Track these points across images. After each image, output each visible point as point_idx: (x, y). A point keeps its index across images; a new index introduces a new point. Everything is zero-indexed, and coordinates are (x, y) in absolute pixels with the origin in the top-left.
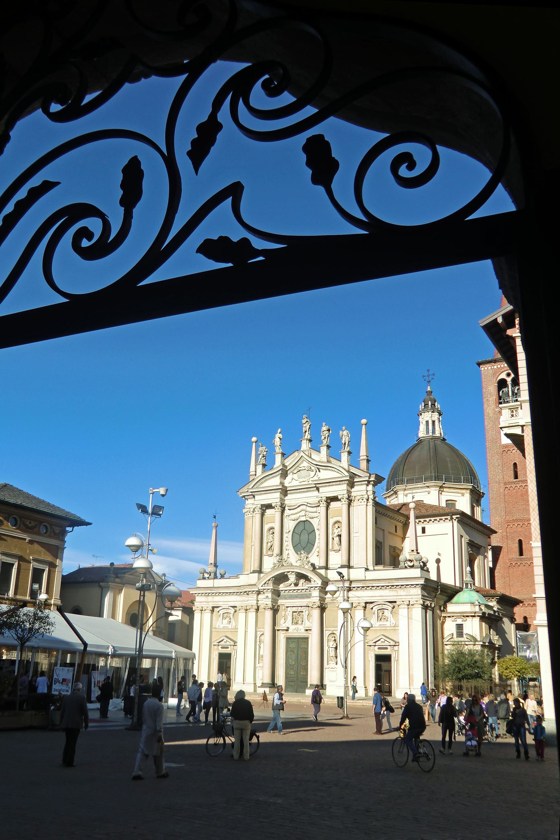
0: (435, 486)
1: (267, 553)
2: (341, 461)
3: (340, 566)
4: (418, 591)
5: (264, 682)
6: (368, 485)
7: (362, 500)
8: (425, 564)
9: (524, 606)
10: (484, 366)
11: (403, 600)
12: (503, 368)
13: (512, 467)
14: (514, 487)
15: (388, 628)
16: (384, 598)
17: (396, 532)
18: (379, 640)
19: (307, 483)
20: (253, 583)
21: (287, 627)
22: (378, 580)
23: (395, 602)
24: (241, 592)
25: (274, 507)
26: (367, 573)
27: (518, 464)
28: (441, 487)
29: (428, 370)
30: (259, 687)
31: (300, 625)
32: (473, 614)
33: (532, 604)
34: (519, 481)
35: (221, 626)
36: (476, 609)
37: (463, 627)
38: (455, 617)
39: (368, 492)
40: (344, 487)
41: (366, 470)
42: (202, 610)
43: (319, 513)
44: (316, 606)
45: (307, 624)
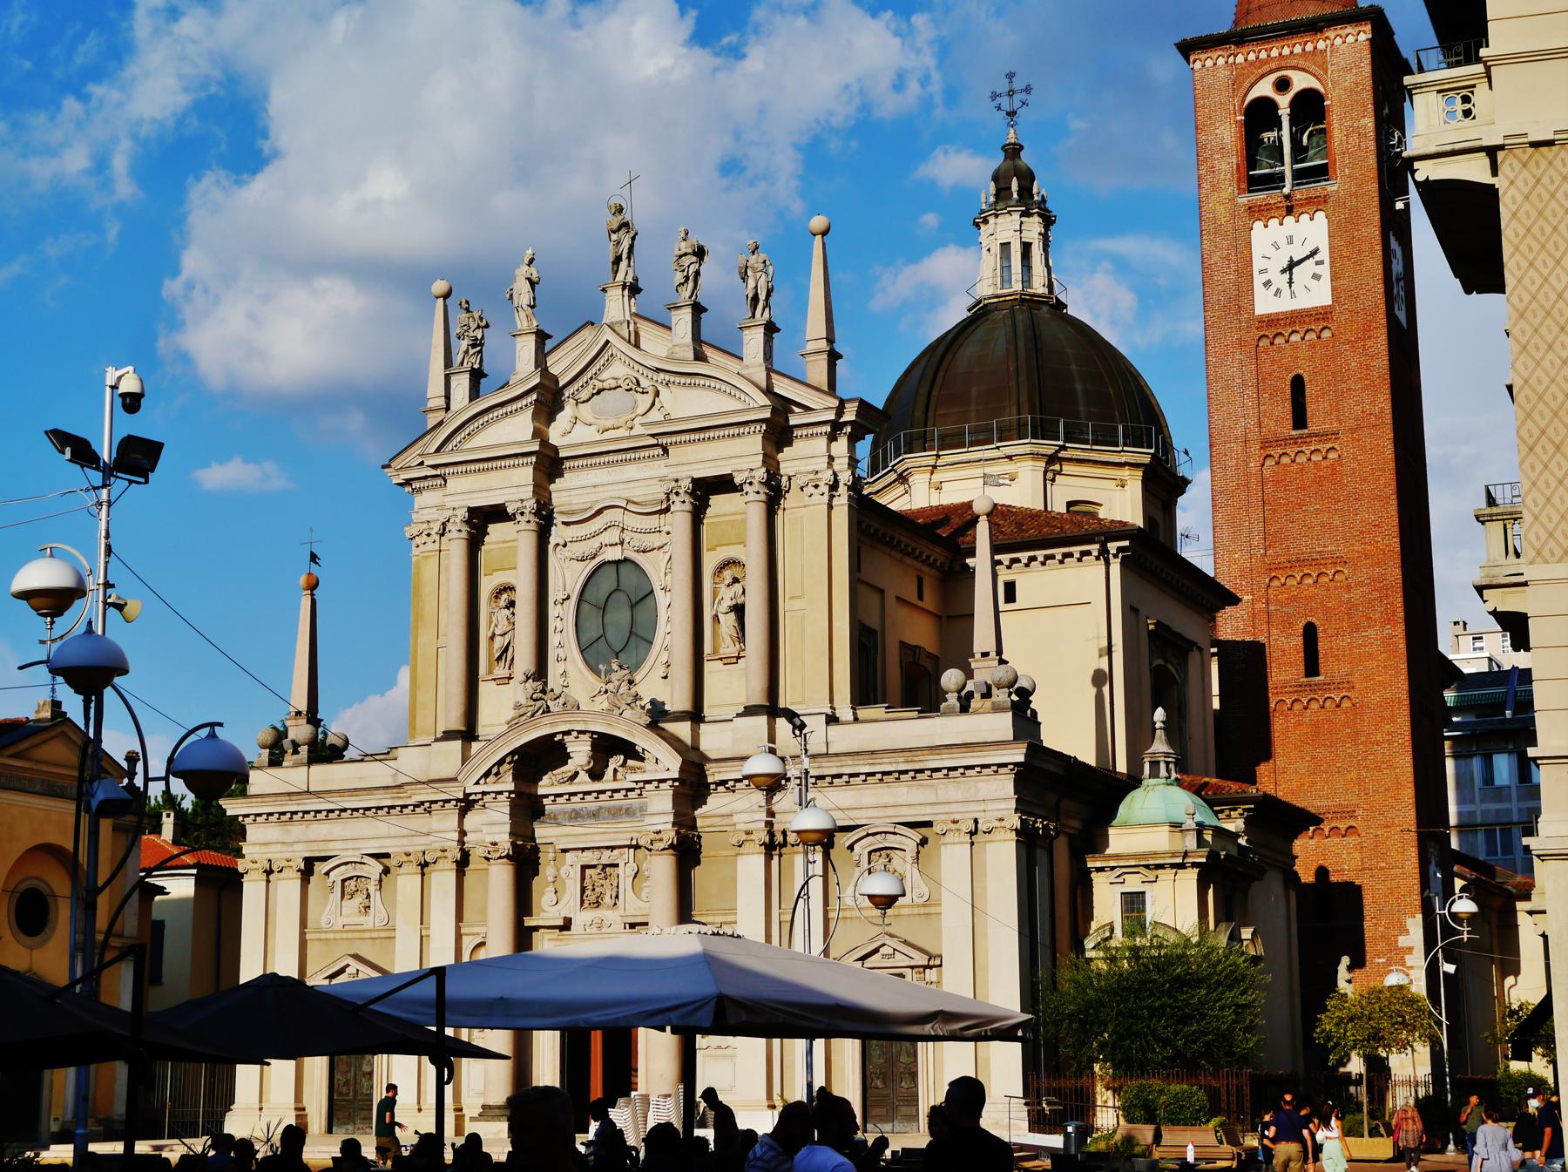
0: (1035, 456)
1: (490, 672)
2: (741, 359)
3: (741, 710)
4: (1004, 786)
5: (491, 1102)
6: (832, 438)
7: (816, 486)
8: (1025, 694)
9: (1321, 834)
10: (1203, 56)
11: (957, 817)
12: (1265, 62)
13: (1288, 391)
14: (1293, 455)
16: (891, 812)
17: (921, 597)
18: (876, 951)
19: (626, 434)
20: (444, 775)
21: (565, 918)
22: (873, 752)
23: (929, 824)
24: (406, 806)
25: (514, 514)
26: (833, 729)
27: (1306, 379)
28: (1052, 459)
29: (1010, 76)
30: (472, 1119)
31: (608, 908)
32: (1179, 860)
33: (1343, 826)
34: (1310, 436)
35: (340, 922)
36: (1187, 844)
37: (1144, 902)
38: (1118, 872)
39: (837, 461)
40: (753, 444)
41: (826, 388)
42: (269, 872)
43: (668, 533)
44: (661, 845)
45: (632, 906)
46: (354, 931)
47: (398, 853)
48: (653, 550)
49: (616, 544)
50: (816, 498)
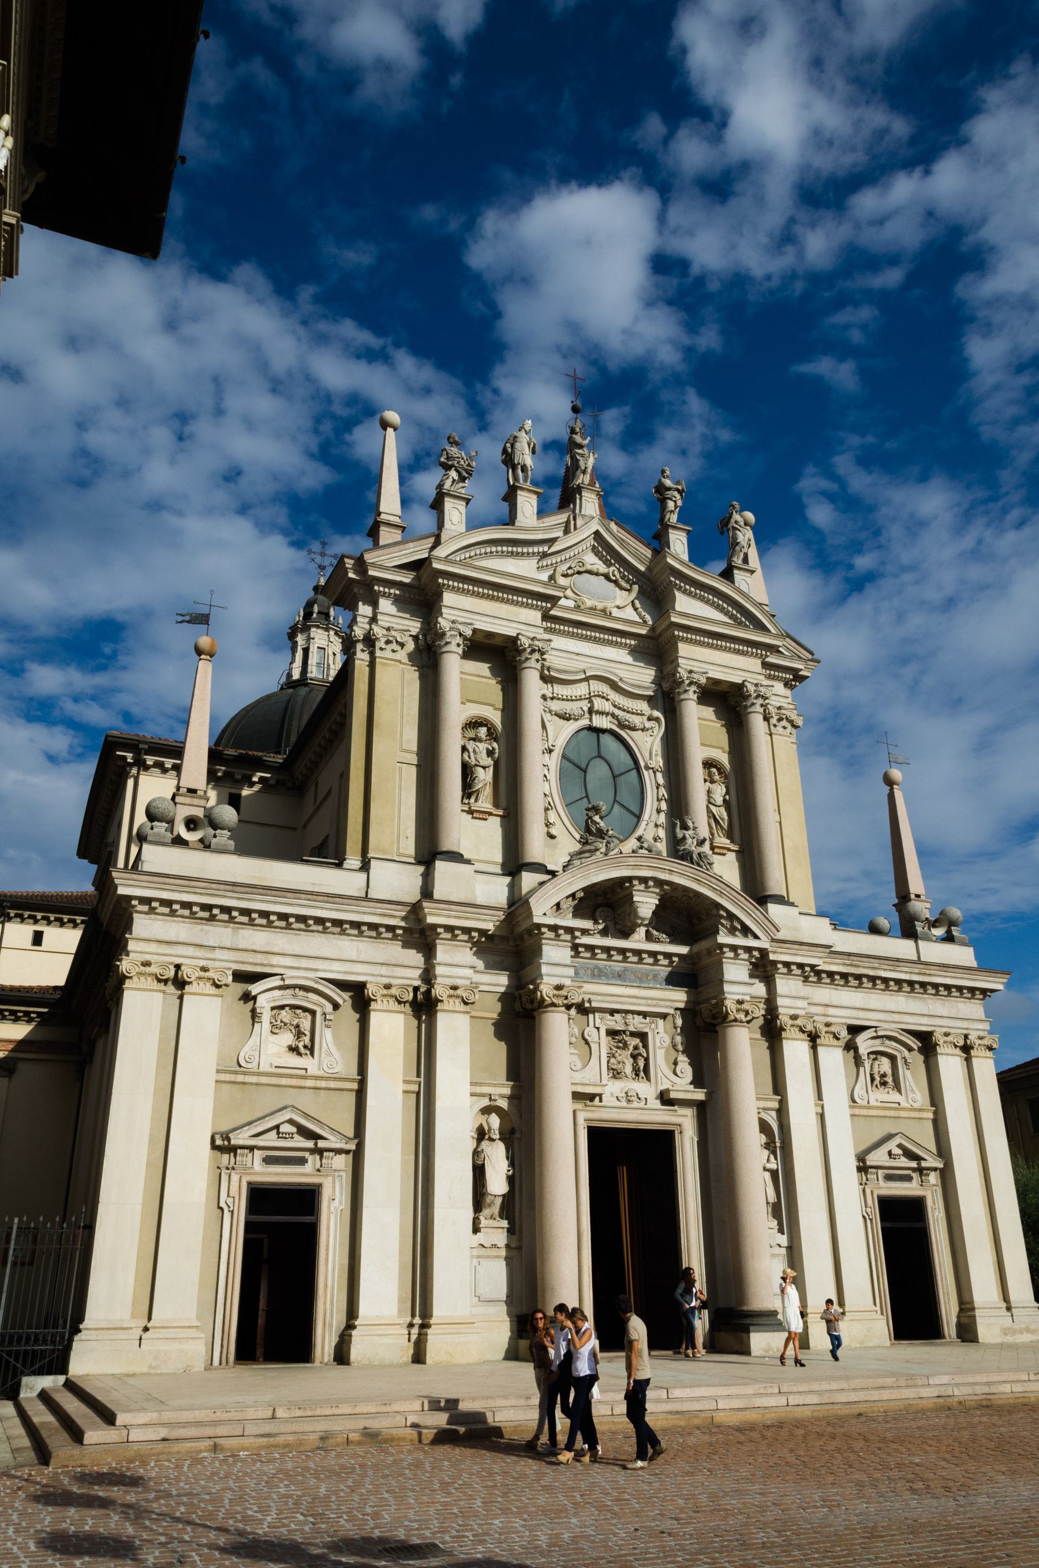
15: (903, 1114)
16: (897, 1017)
22: (898, 960)
46: (291, 1076)
47: (377, 984)
48: (637, 730)
49: (607, 714)
50: (780, 729)
